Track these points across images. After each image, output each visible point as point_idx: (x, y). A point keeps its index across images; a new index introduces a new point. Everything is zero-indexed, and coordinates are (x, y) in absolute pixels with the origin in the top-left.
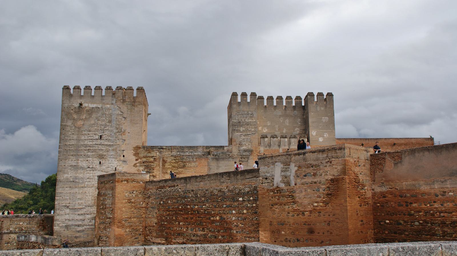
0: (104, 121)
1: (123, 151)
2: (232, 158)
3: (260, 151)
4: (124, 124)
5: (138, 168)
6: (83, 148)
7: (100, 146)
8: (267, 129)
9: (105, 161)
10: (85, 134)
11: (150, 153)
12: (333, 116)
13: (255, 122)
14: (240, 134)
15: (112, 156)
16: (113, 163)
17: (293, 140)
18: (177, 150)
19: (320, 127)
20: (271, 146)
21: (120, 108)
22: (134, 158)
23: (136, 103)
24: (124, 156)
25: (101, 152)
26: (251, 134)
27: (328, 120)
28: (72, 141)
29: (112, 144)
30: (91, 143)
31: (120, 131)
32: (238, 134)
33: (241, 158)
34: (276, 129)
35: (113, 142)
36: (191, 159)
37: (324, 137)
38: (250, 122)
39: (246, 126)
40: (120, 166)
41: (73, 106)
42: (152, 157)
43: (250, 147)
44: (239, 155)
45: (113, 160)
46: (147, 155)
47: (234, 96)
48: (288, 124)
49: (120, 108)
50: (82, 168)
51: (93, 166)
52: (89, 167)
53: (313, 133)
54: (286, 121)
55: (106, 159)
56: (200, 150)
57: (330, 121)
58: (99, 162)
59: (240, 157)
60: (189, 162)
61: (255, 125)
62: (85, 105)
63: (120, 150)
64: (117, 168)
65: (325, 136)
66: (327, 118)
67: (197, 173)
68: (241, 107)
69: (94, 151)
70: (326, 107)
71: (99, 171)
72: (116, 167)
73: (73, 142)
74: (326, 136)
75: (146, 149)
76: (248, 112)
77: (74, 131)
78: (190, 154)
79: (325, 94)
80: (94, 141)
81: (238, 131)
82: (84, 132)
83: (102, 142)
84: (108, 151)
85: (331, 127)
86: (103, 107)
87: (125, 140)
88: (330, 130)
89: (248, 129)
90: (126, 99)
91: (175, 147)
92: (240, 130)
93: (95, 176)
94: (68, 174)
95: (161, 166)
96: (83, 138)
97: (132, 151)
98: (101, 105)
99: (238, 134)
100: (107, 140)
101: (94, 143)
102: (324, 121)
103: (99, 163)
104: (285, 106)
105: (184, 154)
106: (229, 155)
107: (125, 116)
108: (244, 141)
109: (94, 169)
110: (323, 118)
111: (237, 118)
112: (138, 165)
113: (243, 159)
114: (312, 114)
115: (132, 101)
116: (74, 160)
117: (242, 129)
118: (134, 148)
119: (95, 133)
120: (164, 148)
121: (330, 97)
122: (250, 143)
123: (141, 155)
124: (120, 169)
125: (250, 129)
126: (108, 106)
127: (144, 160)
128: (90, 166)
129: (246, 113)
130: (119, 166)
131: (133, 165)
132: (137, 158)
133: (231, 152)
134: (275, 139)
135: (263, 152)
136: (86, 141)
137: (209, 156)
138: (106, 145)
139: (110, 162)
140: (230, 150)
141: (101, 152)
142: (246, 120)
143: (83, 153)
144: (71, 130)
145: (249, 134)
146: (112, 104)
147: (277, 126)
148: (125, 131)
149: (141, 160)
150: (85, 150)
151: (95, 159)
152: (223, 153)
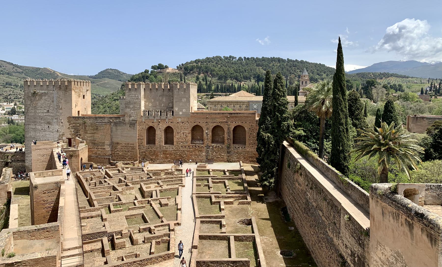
5: (70, 130)
7: (48, 117)
10: (39, 109)
15: (55, 123)
22: (68, 124)
30: (43, 115)
31: (59, 107)
35: (55, 114)
42: (78, 123)
65: (184, 111)
66: (185, 99)
81: (129, 108)
94: (31, 133)
95: (84, 129)
109: (45, 131)
112: (70, 128)
118: (67, 118)
123: (72, 122)
125: (136, 106)
127: (74, 125)
131: (67, 128)
133: (124, 121)
138: (52, 116)
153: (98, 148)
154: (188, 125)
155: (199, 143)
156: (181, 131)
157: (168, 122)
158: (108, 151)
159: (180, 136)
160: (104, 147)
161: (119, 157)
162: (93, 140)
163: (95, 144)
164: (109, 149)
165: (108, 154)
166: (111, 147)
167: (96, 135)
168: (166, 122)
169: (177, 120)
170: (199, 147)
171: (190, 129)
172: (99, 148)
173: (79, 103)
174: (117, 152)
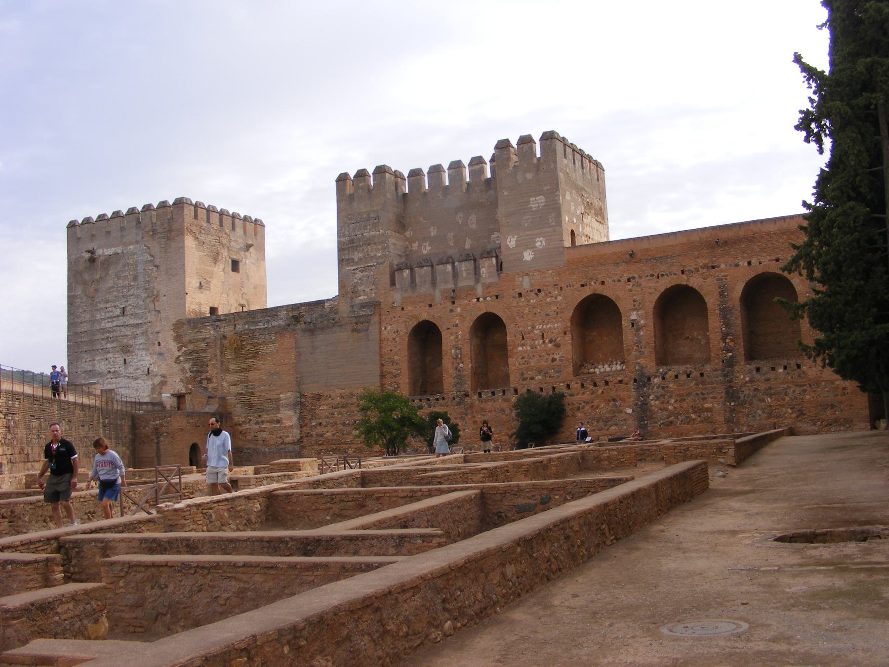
0: (126, 277)
1: (158, 333)
2: (338, 326)
3: (394, 303)
4: (157, 278)
5: (182, 365)
6: (99, 336)
7: (123, 329)
8: (429, 246)
9: (131, 357)
10: (101, 309)
11: (201, 332)
12: (556, 191)
13: (383, 234)
14: (352, 268)
15: (141, 347)
16: (144, 360)
17: (463, 266)
18: (245, 320)
19: (526, 225)
20: (418, 287)
21: (149, 248)
22: (174, 345)
23: (173, 234)
24: (159, 343)
25: (125, 341)
26: (375, 264)
27: (544, 204)
28: (84, 324)
29: (140, 322)
30: (110, 325)
32: (349, 268)
33: (356, 324)
34: (450, 242)
35: (141, 318)
36: (267, 337)
37: (536, 247)
38: (374, 236)
39: (364, 247)
40: (153, 364)
41: (83, 257)
42: (204, 339)
43: (374, 295)
44: (351, 317)
45: (144, 353)
46: (196, 337)
47: (341, 183)
48: (474, 227)
49: (149, 248)
50: (100, 374)
51: (115, 368)
52: (109, 372)
53: (508, 243)
54: (471, 220)
55: (134, 354)
56: (283, 314)
57: (547, 205)
58: (123, 359)
59: (355, 320)
60: (264, 343)
61: (382, 243)
62: (99, 252)
63: (152, 333)
64: (150, 369)
65: (538, 244)
66: (541, 199)
67: (279, 365)
68: (355, 204)
69: (115, 339)
70: (538, 170)
71: (124, 377)
72: (148, 366)
73: (85, 327)
74: (541, 245)
75: (192, 325)
76: (368, 215)
77: (85, 306)
78: (266, 326)
79: (514, 142)
80: (115, 319)
81: (350, 261)
82: (100, 306)
83: (126, 320)
84: (135, 338)
85: (551, 221)
86: (125, 252)
87: (159, 312)
88: (549, 227)
89: (370, 253)
90: (158, 227)
91: (241, 314)
92: (353, 259)
93: (119, 388)
95: (219, 358)
96: (98, 316)
97: (172, 332)
98: (121, 248)
99: (349, 268)
100: (132, 315)
101: (114, 324)
102: (535, 207)
103: (122, 362)
104: (468, 184)
105: (257, 327)
106: (334, 320)
107: (157, 262)
108: (363, 284)
109: (116, 375)
110: (533, 201)
111: (347, 233)
112: (182, 358)
113: (360, 326)
114: (506, 194)
115: (167, 229)
116: (89, 360)
117: (357, 256)
119: (114, 304)
120: (222, 318)
121: (548, 143)
122: (373, 287)
123: (186, 339)
124: (155, 370)
125: (372, 254)
126: (132, 247)
127: (191, 347)
128: (111, 368)
129: (365, 216)
130: (152, 365)
132: (179, 345)
133: (336, 313)
134: (426, 268)
135: (400, 304)
136: (103, 322)
137: (299, 327)
139: (139, 358)
140: (336, 308)
141: (125, 341)
142: (364, 234)
143: (99, 347)
144: (82, 305)
145: (371, 266)
146: (137, 242)
147: (450, 235)
148: (158, 292)
149: (186, 349)
150: (103, 339)
151: (117, 356)
152: (321, 316)
153: (260, 420)
154: (560, 298)
155: (608, 369)
156: (533, 328)
157: (485, 298)
158: (291, 427)
159: (532, 348)
160: (279, 415)
161: (324, 447)
162: (247, 393)
163: (250, 406)
164: (294, 421)
165: (290, 439)
166: (298, 412)
167: (252, 375)
168: (478, 299)
169: (517, 283)
170: (607, 383)
171: (569, 314)
172: (263, 422)
173: (213, 281)
174: (320, 430)
